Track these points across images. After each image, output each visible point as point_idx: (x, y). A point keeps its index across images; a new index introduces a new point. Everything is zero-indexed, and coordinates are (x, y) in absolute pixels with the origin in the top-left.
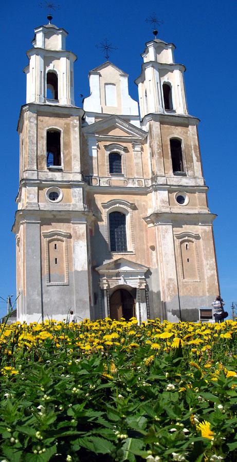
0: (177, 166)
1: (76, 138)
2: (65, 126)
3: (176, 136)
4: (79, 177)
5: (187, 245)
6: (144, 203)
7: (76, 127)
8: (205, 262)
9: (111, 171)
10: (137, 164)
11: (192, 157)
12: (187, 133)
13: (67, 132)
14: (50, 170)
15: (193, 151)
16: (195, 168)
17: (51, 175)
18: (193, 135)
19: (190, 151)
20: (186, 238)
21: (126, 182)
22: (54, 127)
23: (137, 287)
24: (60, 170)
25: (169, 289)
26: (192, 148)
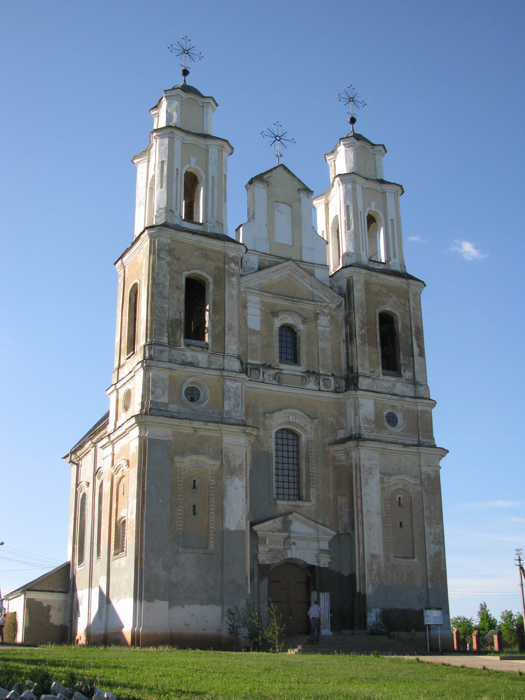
1: (232, 295)
2: (216, 272)
3: (388, 309)
4: (236, 365)
5: (399, 498)
6: (331, 419)
8: (427, 530)
10: (324, 349)
12: (404, 305)
21: (304, 380)
22: (198, 272)
23: (316, 564)
25: (371, 573)
26: (413, 332)
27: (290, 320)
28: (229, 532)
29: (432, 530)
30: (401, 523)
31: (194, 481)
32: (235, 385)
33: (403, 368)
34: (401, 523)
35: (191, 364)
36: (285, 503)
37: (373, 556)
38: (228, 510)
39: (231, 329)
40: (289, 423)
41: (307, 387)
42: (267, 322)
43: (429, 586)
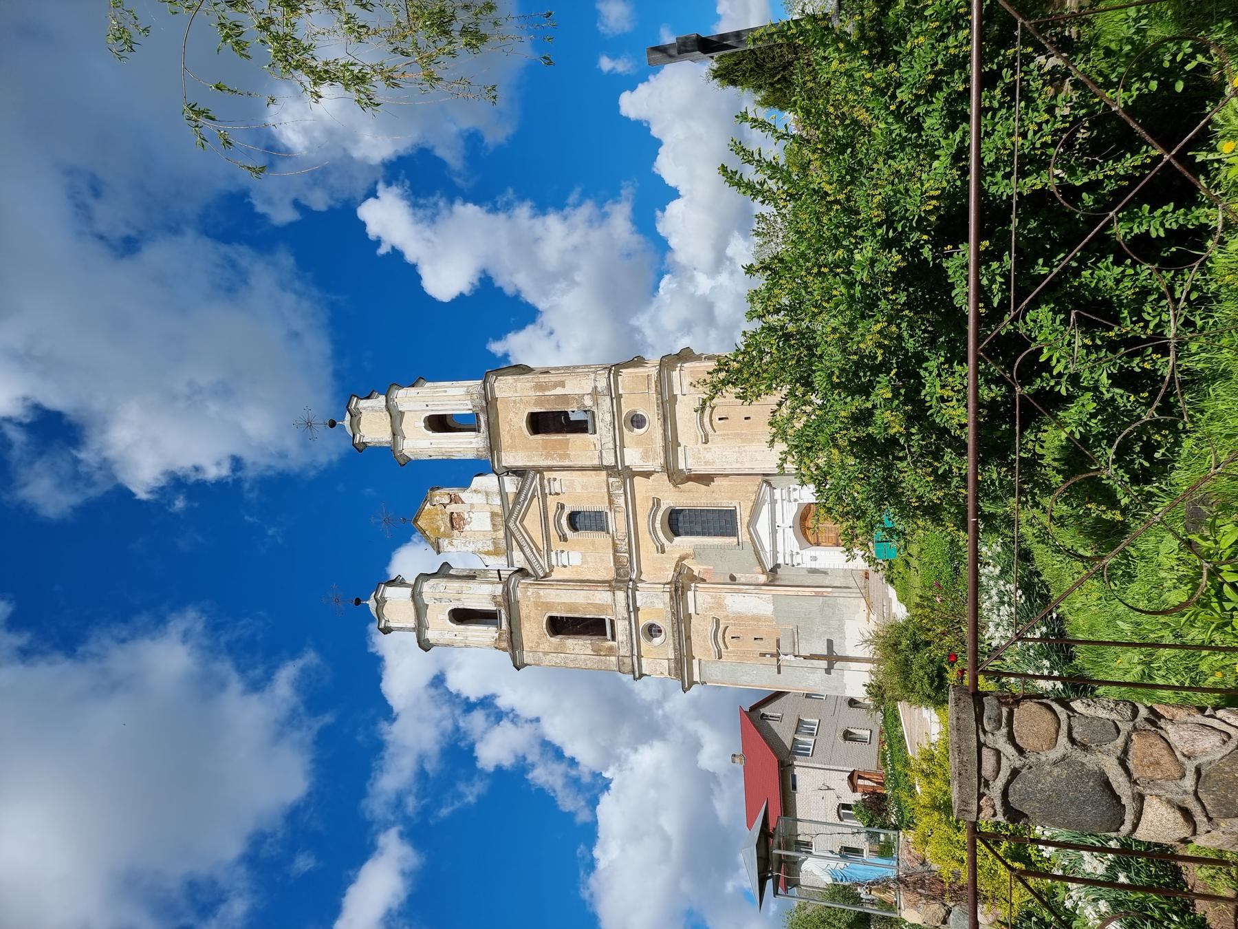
4: (621, 595)
5: (720, 419)
9: (585, 430)
12: (515, 402)
13: (549, 606)
14: (613, 638)
17: (621, 636)
19: (547, 399)
22: (544, 626)
24: (612, 622)
26: (541, 394)
28: (775, 610)
30: (746, 418)
31: (733, 638)
34: (746, 418)
38: (755, 611)
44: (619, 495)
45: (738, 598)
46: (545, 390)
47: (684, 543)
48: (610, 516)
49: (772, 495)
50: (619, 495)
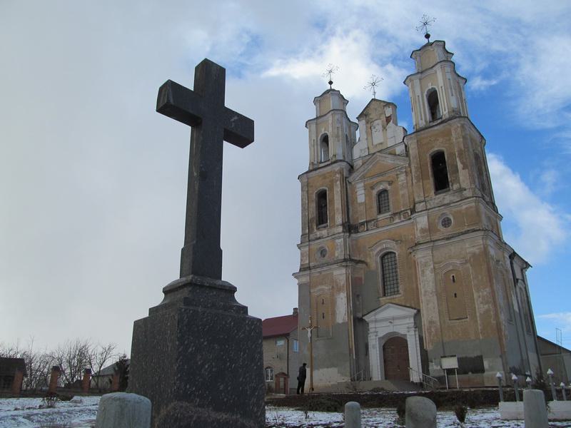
0: (441, 182)
1: (338, 192)
4: (340, 229)
7: (337, 181)
8: (476, 295)
10: (403, 195)
11: (457, 166)
12: (450, 140)
13: (331, 188)
15: (457, 159)
16: (461, 178)
18: (456, 139)
20: (451, 268)
25: (430, 335)
27: (381, 187)
29: (481, 294)
30: (455, 294)
32: (340, 240)
33: (450, 184)
34: (455, 294)
35: (320, 238)
36: (384, 298)
37: (431, 322)
39: (338, 209)
40: (386, 248)
41: (395, 222)
42: (368, 195)
43: (481, 338)
44: (400, 218)
45: (345, 300)
46: (459, 157)
47: (374, 262)
48: (387, 215)
49: (410, 317)
50: (400, 218)
